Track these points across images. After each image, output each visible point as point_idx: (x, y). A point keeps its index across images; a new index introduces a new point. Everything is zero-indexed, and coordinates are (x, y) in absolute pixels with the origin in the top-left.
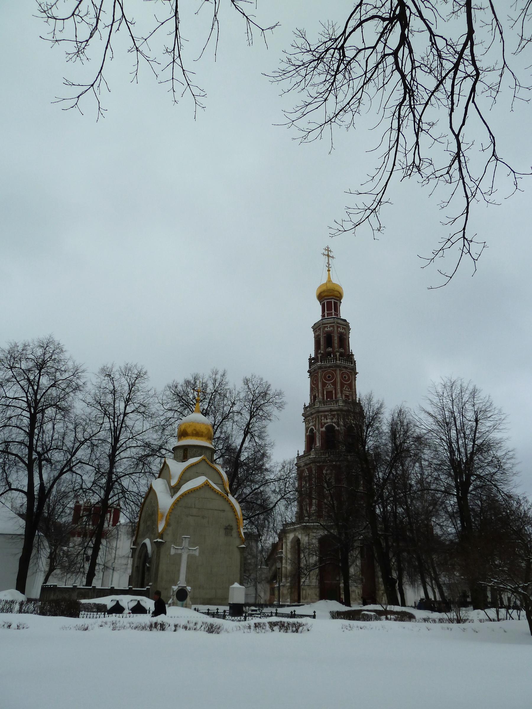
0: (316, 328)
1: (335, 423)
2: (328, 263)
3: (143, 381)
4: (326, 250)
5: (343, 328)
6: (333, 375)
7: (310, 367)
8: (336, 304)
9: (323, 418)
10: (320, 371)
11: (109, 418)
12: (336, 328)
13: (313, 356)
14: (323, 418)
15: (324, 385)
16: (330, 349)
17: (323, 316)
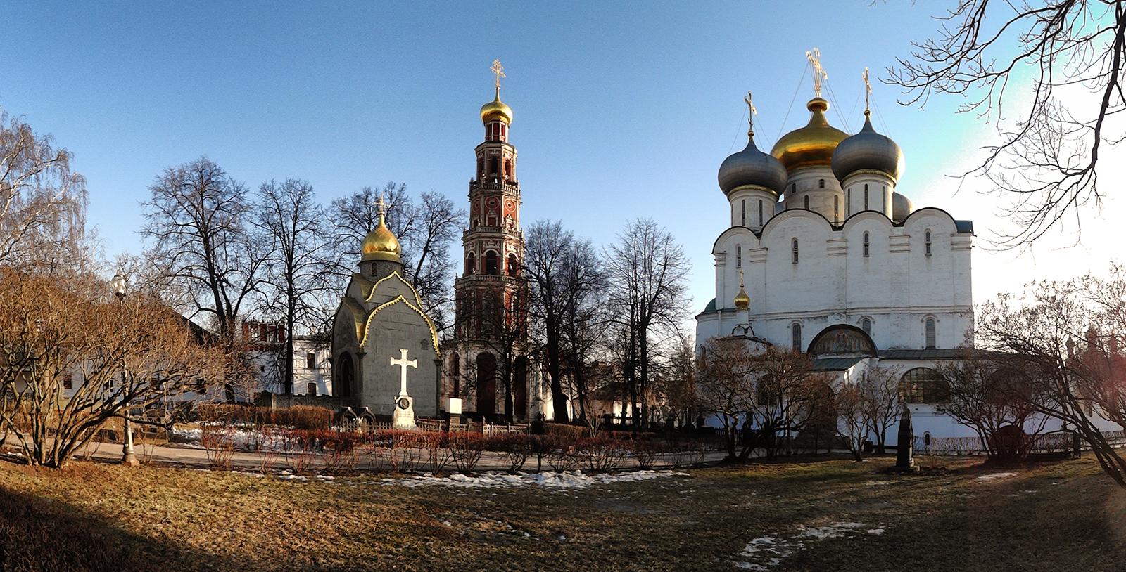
1: (496, 249)
3: (309, 198)
7: (471, 191)
9: (484, 243)
10: (483, 196)
11: (280, 237)
13: (475, 180)
14: (484, 243)
15: (486, 211)
17: (488, 138)
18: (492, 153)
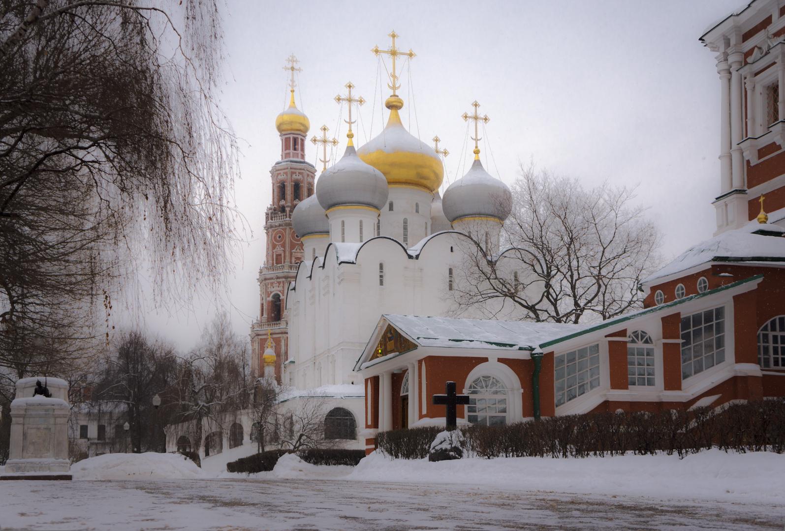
0: (275, 172)
1: (280, 291)
2: (293, 81)
4: (289, 61)
5: (299, 173)
6: (282, 234)
8: (295, 140)
9: (269, 286)
12: (289, 176)
14: (269, 286)
16: (283, 202)
18: (280, 177)
